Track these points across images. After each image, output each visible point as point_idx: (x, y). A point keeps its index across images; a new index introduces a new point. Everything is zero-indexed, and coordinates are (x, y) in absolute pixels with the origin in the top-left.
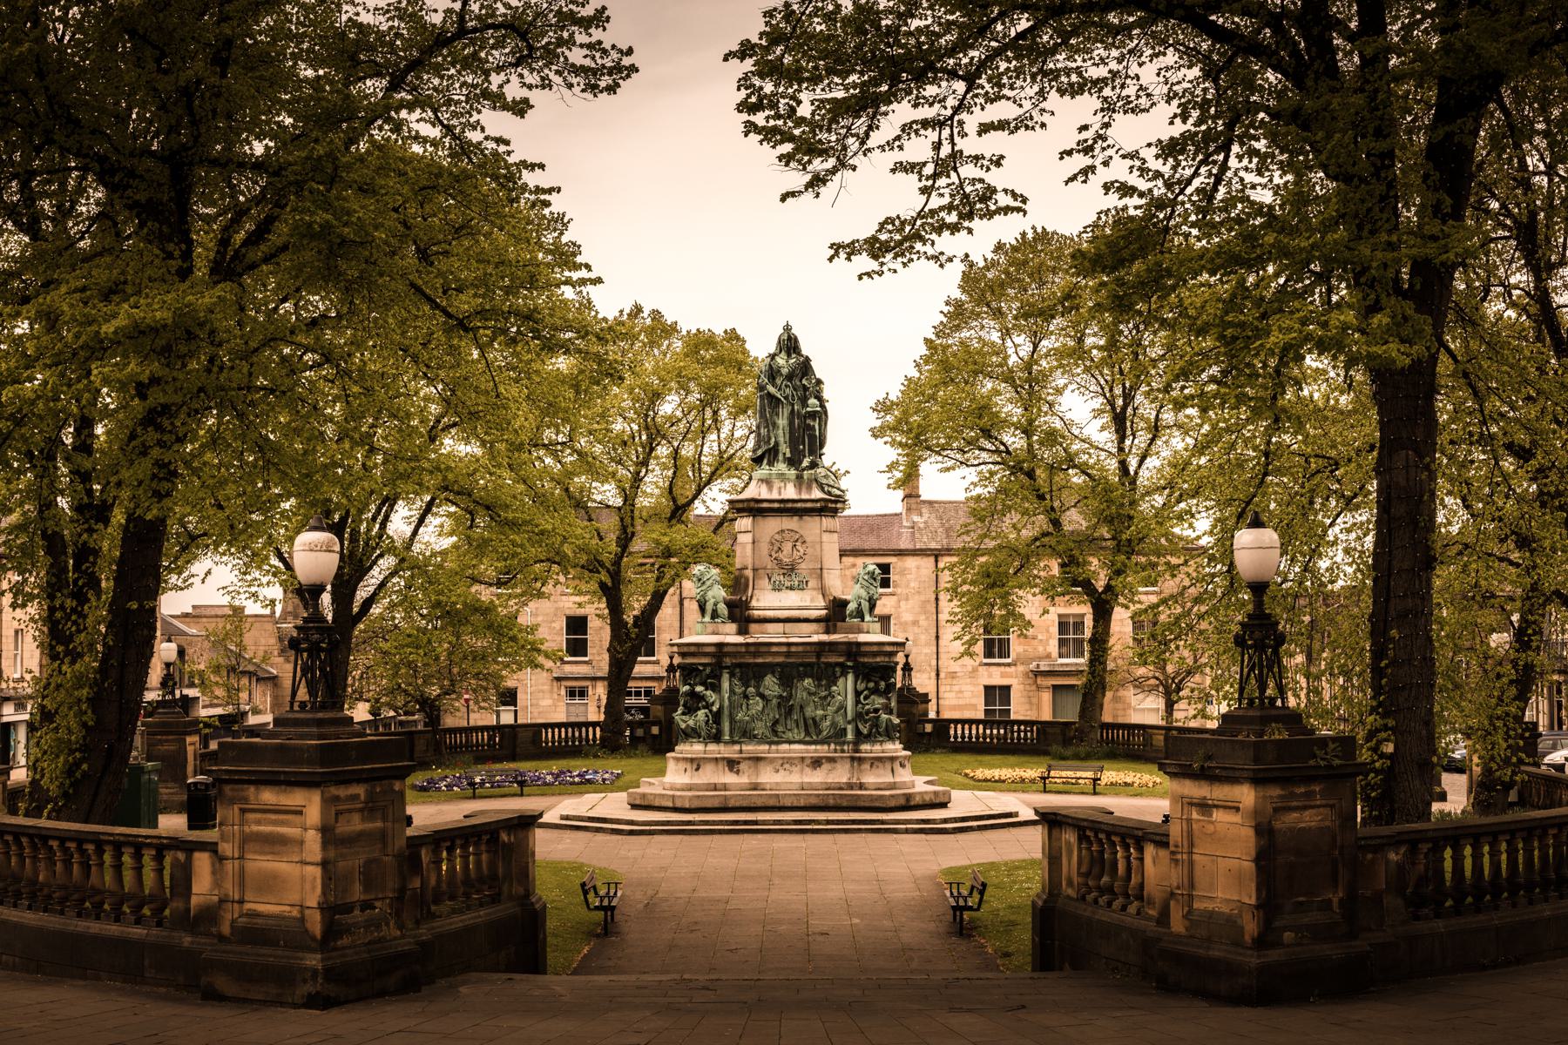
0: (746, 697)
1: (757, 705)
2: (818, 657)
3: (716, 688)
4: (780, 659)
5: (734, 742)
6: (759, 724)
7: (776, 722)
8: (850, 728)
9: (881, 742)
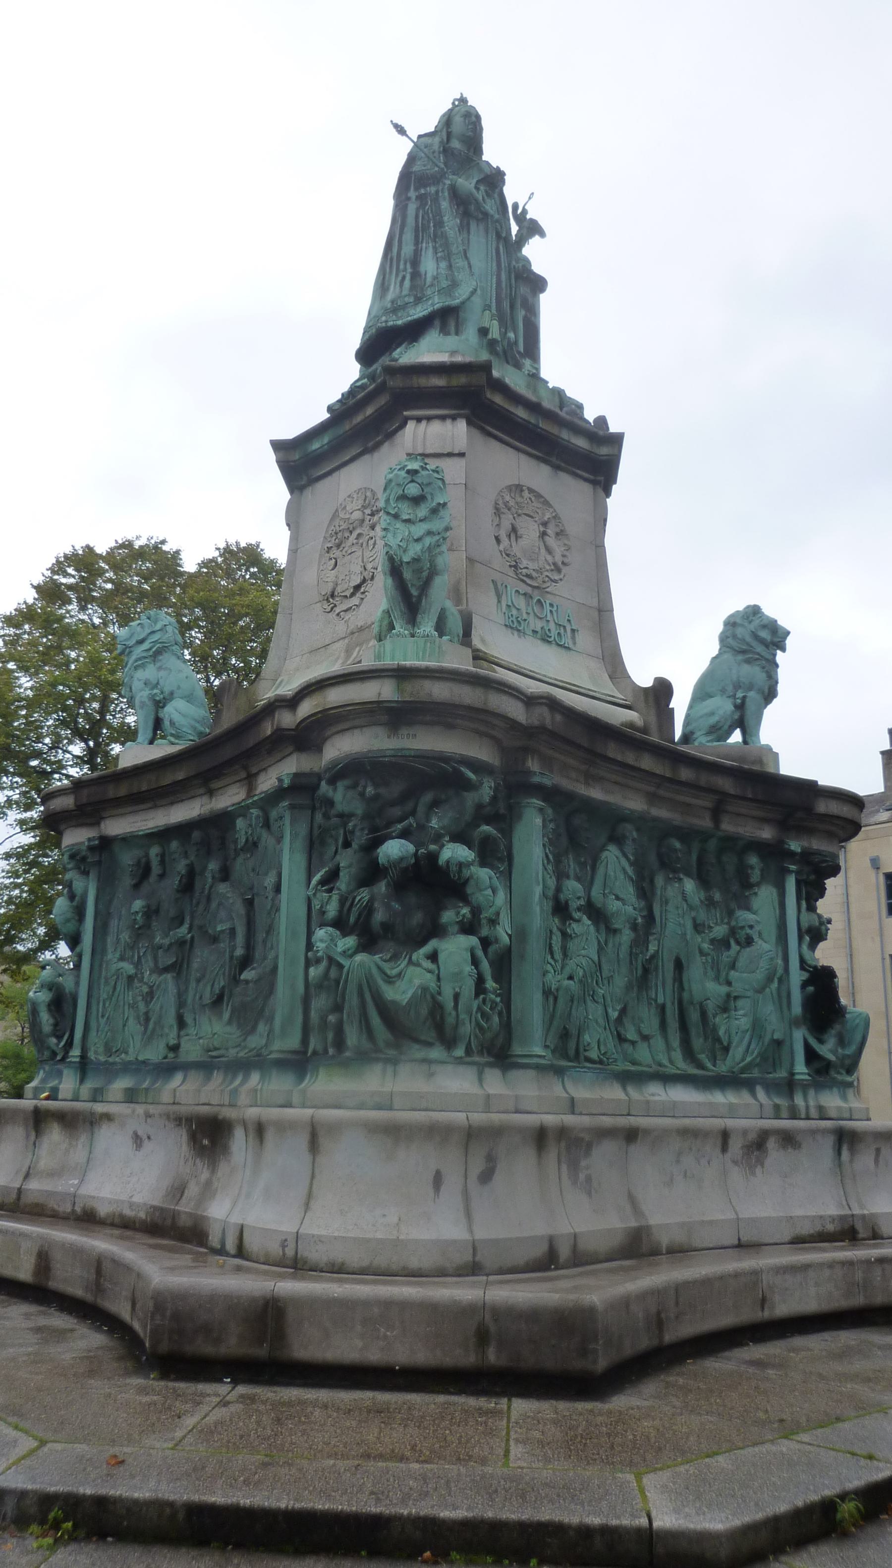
2: (716, 813)
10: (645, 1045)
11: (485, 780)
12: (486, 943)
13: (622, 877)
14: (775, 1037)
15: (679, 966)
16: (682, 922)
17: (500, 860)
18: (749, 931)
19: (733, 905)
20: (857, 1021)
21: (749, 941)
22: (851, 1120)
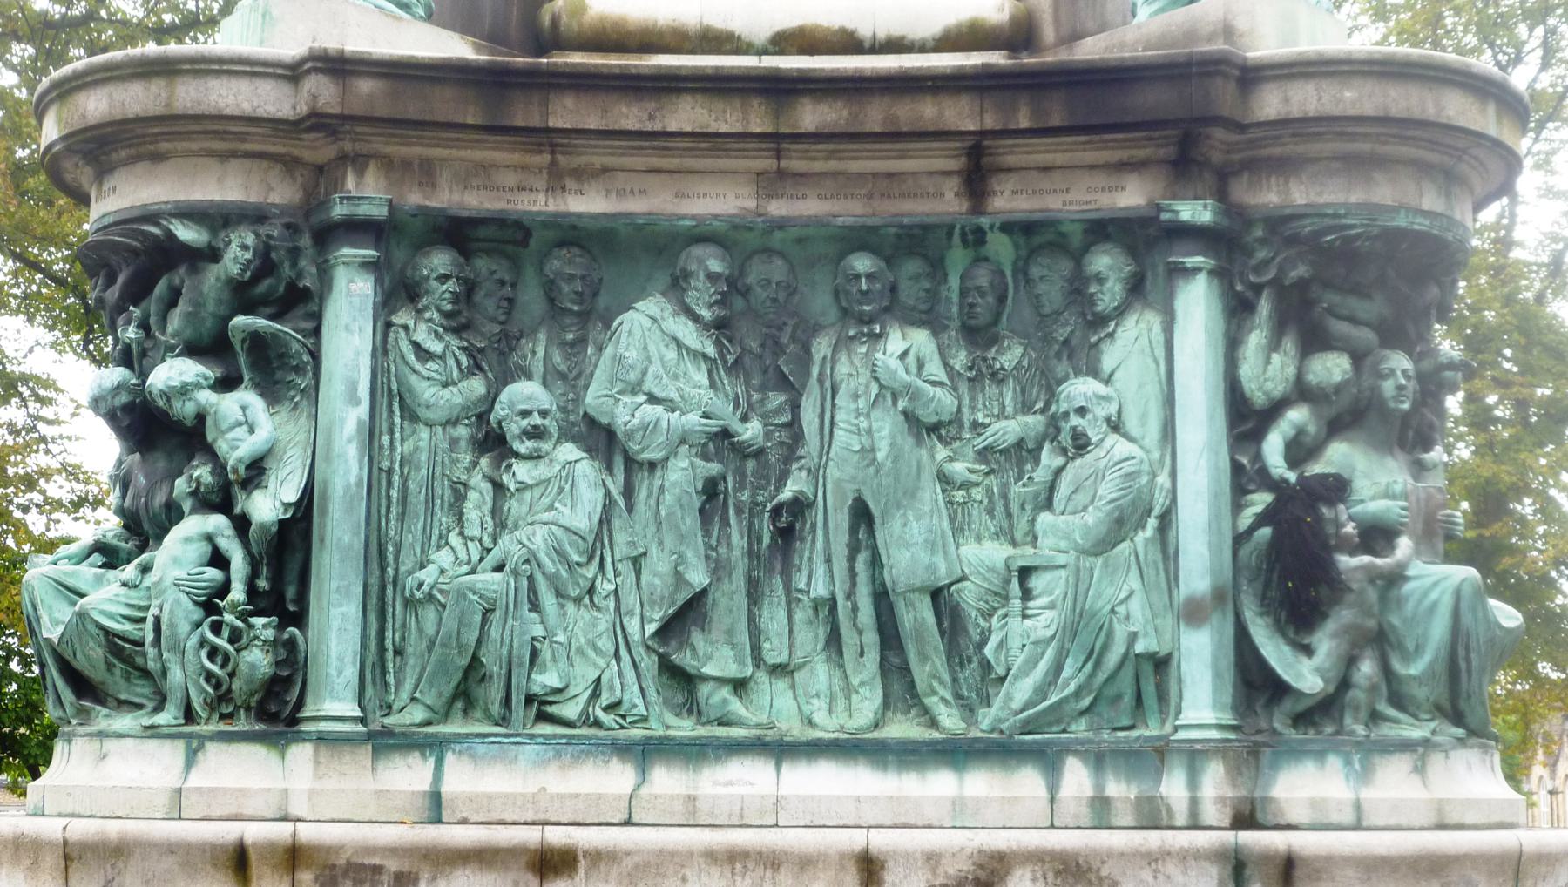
0: (493, 443)
1: (563, 493)
2: (977, 176)
3: (279, 370)
4: (719, 200)
5: (386, 742)
6: (583, 626)
7: (688, 615)
8: (1200, 660)
9: (1420, 750)
10: (781, 685)
11: (232, 236)
12: (242, 524)
13: (671, 354)
14: (1139, 648)
15: (862, 515)
16: (864, 425)
17: (299, 370)
18: (1075, 420)
19: (1062, 368)
20: (1434, 596)
21: (1081, 444)
22: (1357, 827)
